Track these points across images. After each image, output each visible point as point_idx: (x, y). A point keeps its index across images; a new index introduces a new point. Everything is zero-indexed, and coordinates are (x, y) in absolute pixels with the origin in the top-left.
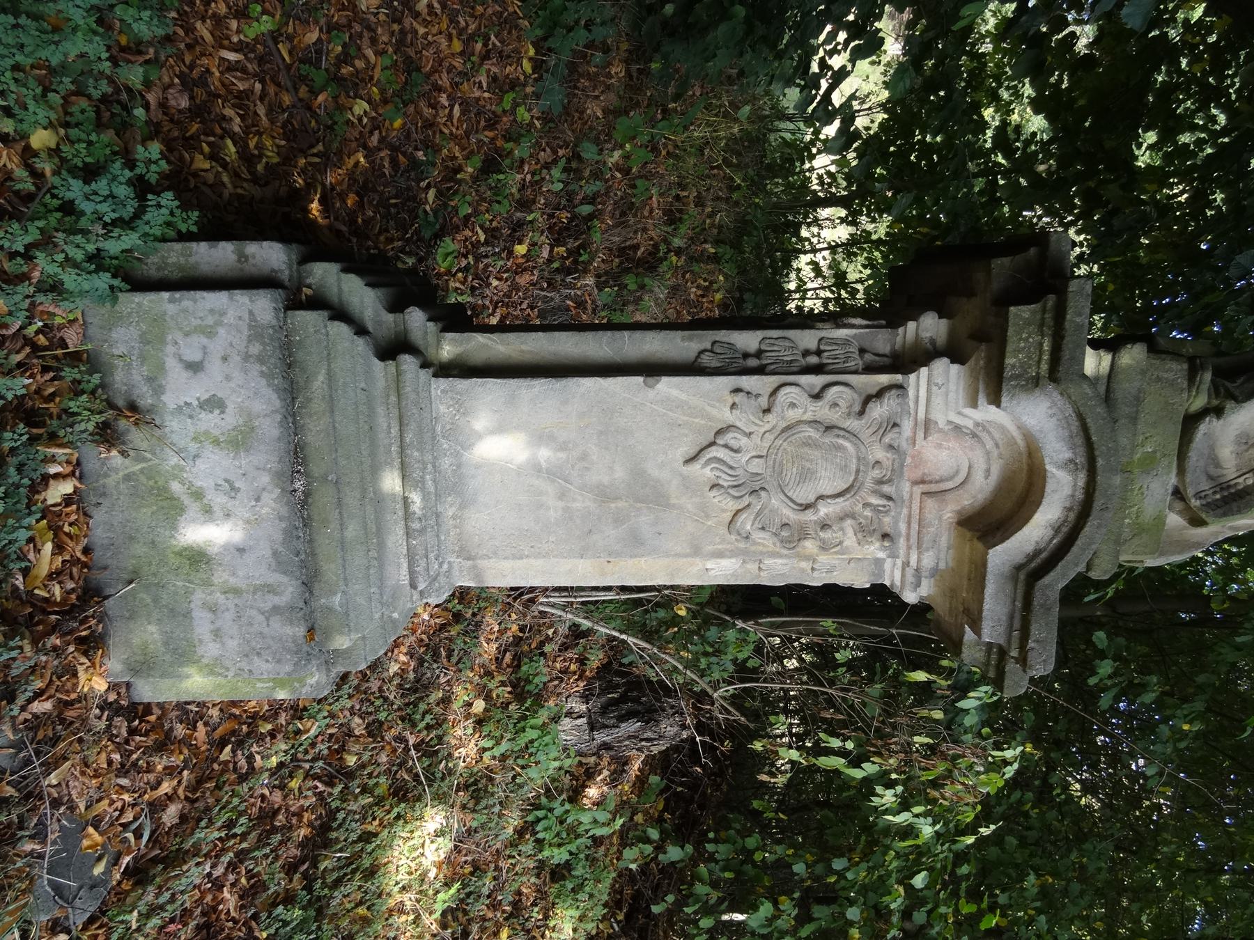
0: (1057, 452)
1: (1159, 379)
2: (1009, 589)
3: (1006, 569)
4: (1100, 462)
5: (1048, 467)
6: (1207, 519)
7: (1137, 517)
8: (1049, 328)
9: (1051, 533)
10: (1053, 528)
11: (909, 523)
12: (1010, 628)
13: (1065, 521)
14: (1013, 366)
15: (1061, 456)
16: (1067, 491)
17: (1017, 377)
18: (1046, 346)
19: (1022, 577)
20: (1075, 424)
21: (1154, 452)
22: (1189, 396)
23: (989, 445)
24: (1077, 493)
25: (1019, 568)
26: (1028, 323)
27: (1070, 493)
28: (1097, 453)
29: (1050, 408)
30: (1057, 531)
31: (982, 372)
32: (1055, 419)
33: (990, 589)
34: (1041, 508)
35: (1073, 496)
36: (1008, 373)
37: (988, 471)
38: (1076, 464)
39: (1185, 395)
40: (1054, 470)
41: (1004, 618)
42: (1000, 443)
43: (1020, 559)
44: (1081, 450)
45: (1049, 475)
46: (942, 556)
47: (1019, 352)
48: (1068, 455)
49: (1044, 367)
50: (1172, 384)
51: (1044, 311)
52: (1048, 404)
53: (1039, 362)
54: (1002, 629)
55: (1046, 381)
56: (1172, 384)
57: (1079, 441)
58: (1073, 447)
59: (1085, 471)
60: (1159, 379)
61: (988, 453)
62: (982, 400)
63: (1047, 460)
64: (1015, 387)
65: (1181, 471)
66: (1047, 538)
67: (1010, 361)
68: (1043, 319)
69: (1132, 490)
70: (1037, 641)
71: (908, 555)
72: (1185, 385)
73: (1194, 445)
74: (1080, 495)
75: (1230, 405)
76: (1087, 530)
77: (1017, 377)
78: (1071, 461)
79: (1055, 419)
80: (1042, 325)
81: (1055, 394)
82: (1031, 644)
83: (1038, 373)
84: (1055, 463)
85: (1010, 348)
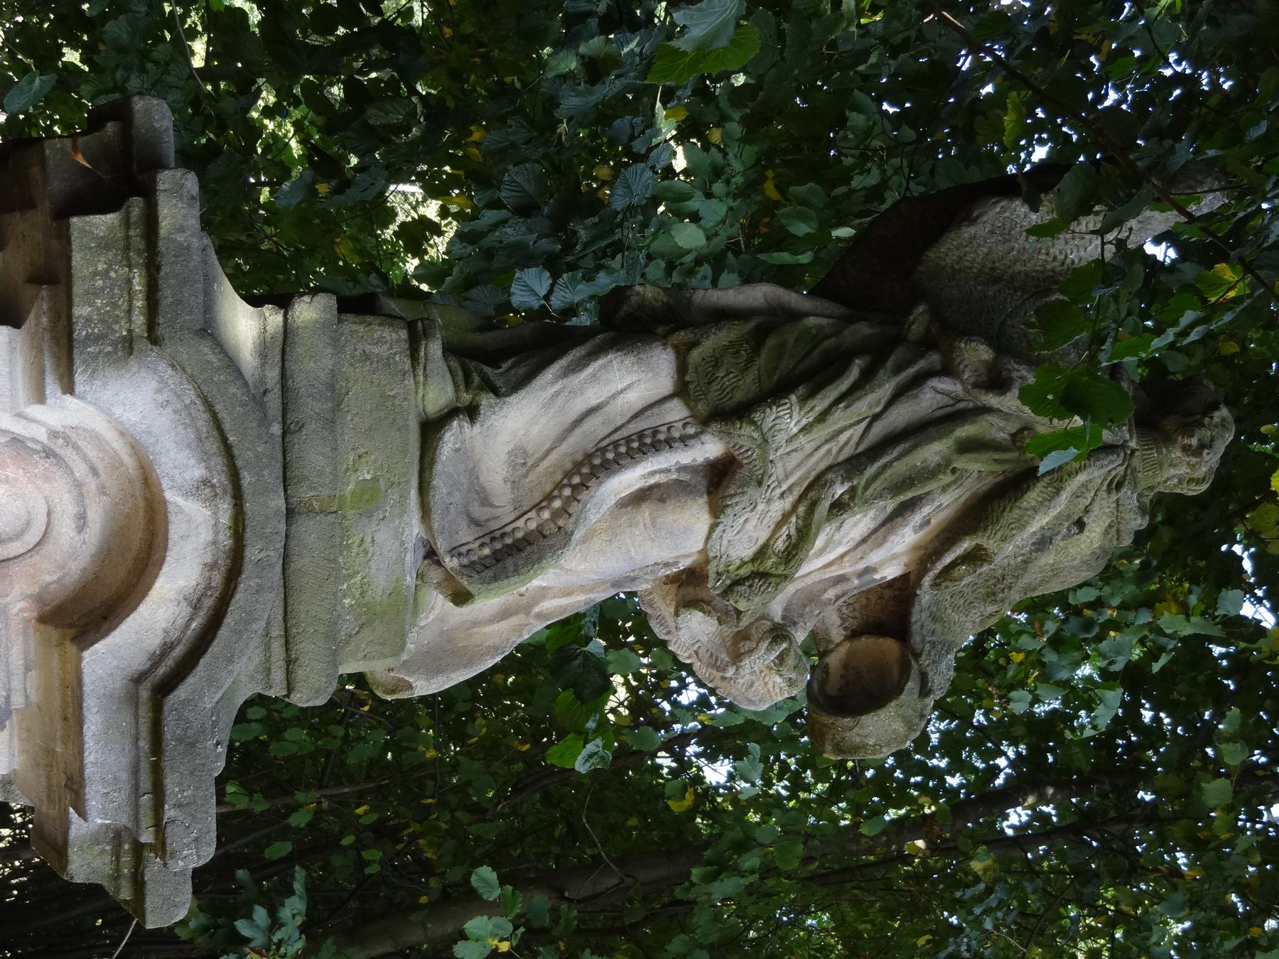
0: (181, 467)
1: (366, 356)
2: (125, 720)
3: (118, 684)
4: (247, 479)
5: (169, 495)
6: (472, 589)
7: (363, 593)
8: (139, 253)
9: (186, 610)
10: (190, 602)
12: (136, 791)
13: (208, 587)
14: (88, 320)
15: (188, 476)
16: (205, 535)
17: (98, 339)
18: (138, 284)
19: (145, 694)
20: (203, 418)
21: (375, 479)
22: (417, 383)
23: (80, 470)
24: (221, 537)
25: (138, 679)
26: (105, 245)
27: (210, 538)
28: (239, 463)
29: (159, 391)
30: (196, 607)
31: (47, 336)
32: (169, 410)
33: (93, 723)
34: (165, 569)
35: (214, 543)
36: (80, 332)
37: (81, 521)
38: (213, 486)
39: (410, 382)
40: (180, 500)
41: (124, 776)
42: (100, 466)
43: (139, 662)
44: (218, 462)
45: (171, 508)
46: (16, 683)
47: (96, 295)
48: (198, 472)
49: (139, 320)
50: (388, 363)
51: (127, 224)
52: (154, 385)
53: (129, 311)
54: (122, 797)
55: (145, 345)
56: (388, 363)
57: (213, 446)
58: (204, 458)
59: (228, 499)
61: (78, 485)
62: (52, 387)
63: (165, 483)
64: (95, 357)
65: (425, 512)
66: (181, 622)
67: (81, 311)
68: (127, 237)
69: (348, 547)
70: (179, 806)
72: (407, 365)
73: (438, 468)
74: (226, 541)
75: (486, 400)
76: (240, 598)
77: (98, 339)
78: (205, 482)
79: (169, 410)
80: (127, 248)
81: (162, 366)
82: (169, 813)
83: (130, 331)
84: (180, 488)
85: (78, 289)
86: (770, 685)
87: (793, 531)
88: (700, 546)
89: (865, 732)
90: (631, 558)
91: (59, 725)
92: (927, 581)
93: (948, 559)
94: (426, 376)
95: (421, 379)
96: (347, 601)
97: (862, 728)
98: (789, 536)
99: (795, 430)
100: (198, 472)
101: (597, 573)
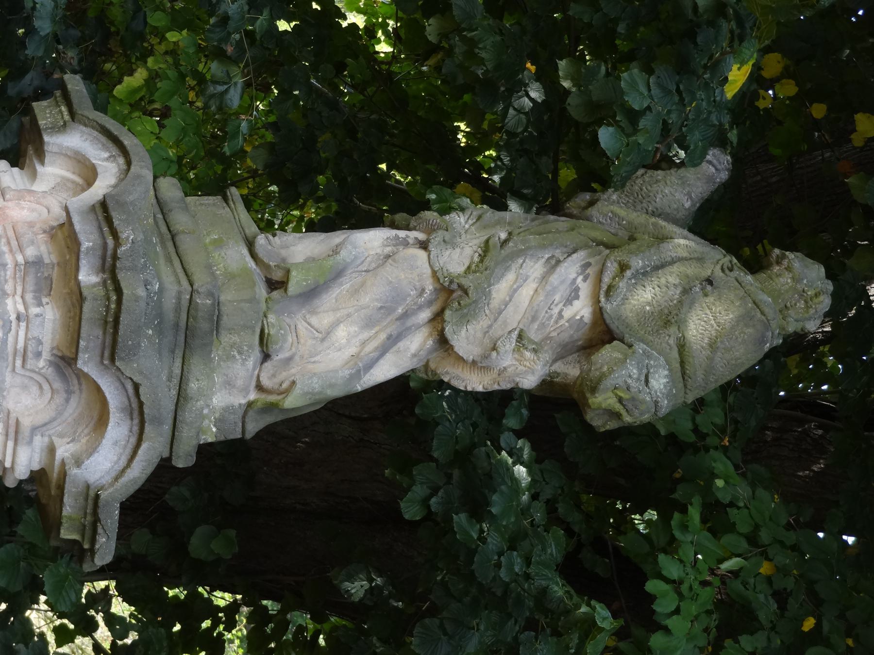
5: (94, 162)
11: (9, 243)
14: (46, 124)
17: (51, 128)
18: (63, 108)
20: (103, 139)
39: (227, 209)
48: (106, 155)
49: (67, 117)
53: (63, 118)
57: (110, 144)
60: (202, 204)
71: (15, 258)
72: (225, 205)
78: (110, 157)
80: (57, 102)
82: (116, 223)
86: (528, 364)
87: (481, 252)
88: (429, 271)
89: (598, 366)
90: (391, 282)
91: (66, 250)
92: (603, 299)
93: (606, 280)
94: (234, 203)
95: (233, 205)
96: (218, 272)
97: (595, 364)
98: (480, 255)
99: (467, 226)
100: (106, 155)
101: (377, 300)
